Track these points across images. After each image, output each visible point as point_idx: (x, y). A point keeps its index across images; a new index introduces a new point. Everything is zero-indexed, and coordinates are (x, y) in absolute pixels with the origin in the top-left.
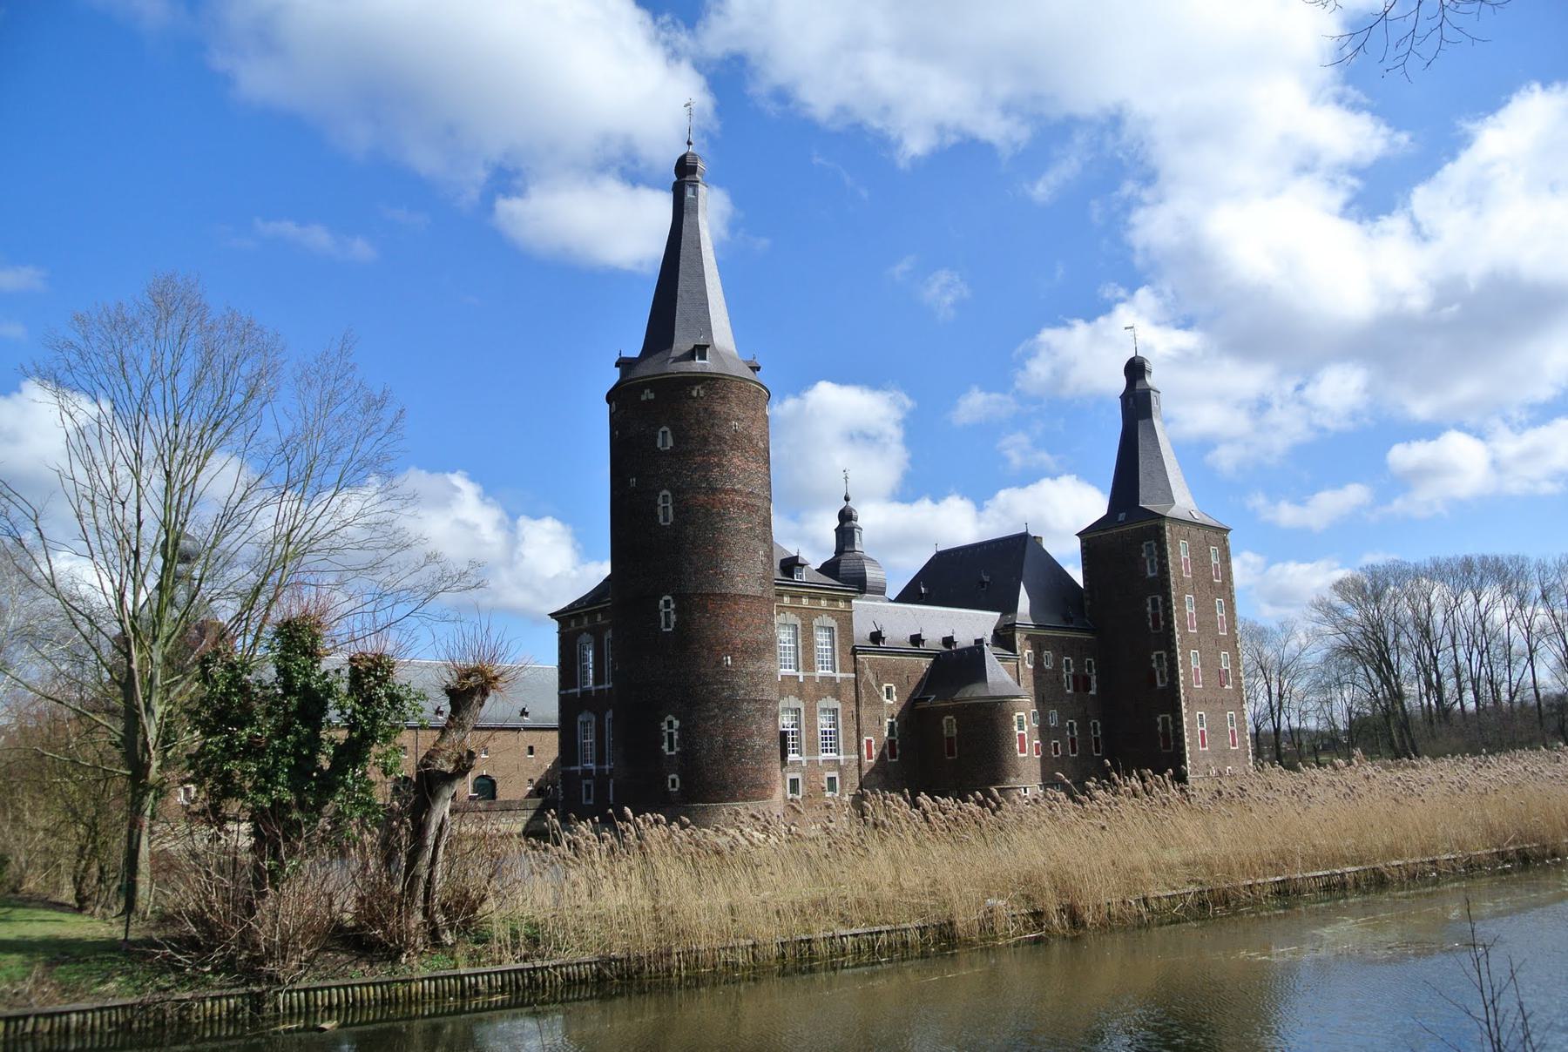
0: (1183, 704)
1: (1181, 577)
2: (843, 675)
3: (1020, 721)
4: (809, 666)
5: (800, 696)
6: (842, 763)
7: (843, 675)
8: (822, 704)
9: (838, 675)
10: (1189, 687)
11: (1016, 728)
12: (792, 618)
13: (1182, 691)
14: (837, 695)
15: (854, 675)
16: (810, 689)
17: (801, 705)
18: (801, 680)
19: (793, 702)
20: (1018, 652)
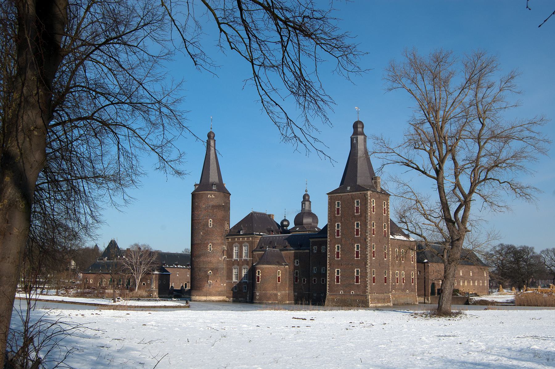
0: (328, 266)
1: (334, 216)
2: (250, 259)
3: (259, 272)
4: (241, 256)
5: (238, 265)
6: (248, 283)
7: (250, 259)
8: (243, 267)
9: (248, 259)
10: (332, 259)
11: (257, 274)
12: (237, 244)
13: (328, 261)
14: (248, 264)
15: (252, 259)
16: (241, 263)
17: (238, 267)
18: (238, 260)
19: (236, 266)
20: (311, 247)
